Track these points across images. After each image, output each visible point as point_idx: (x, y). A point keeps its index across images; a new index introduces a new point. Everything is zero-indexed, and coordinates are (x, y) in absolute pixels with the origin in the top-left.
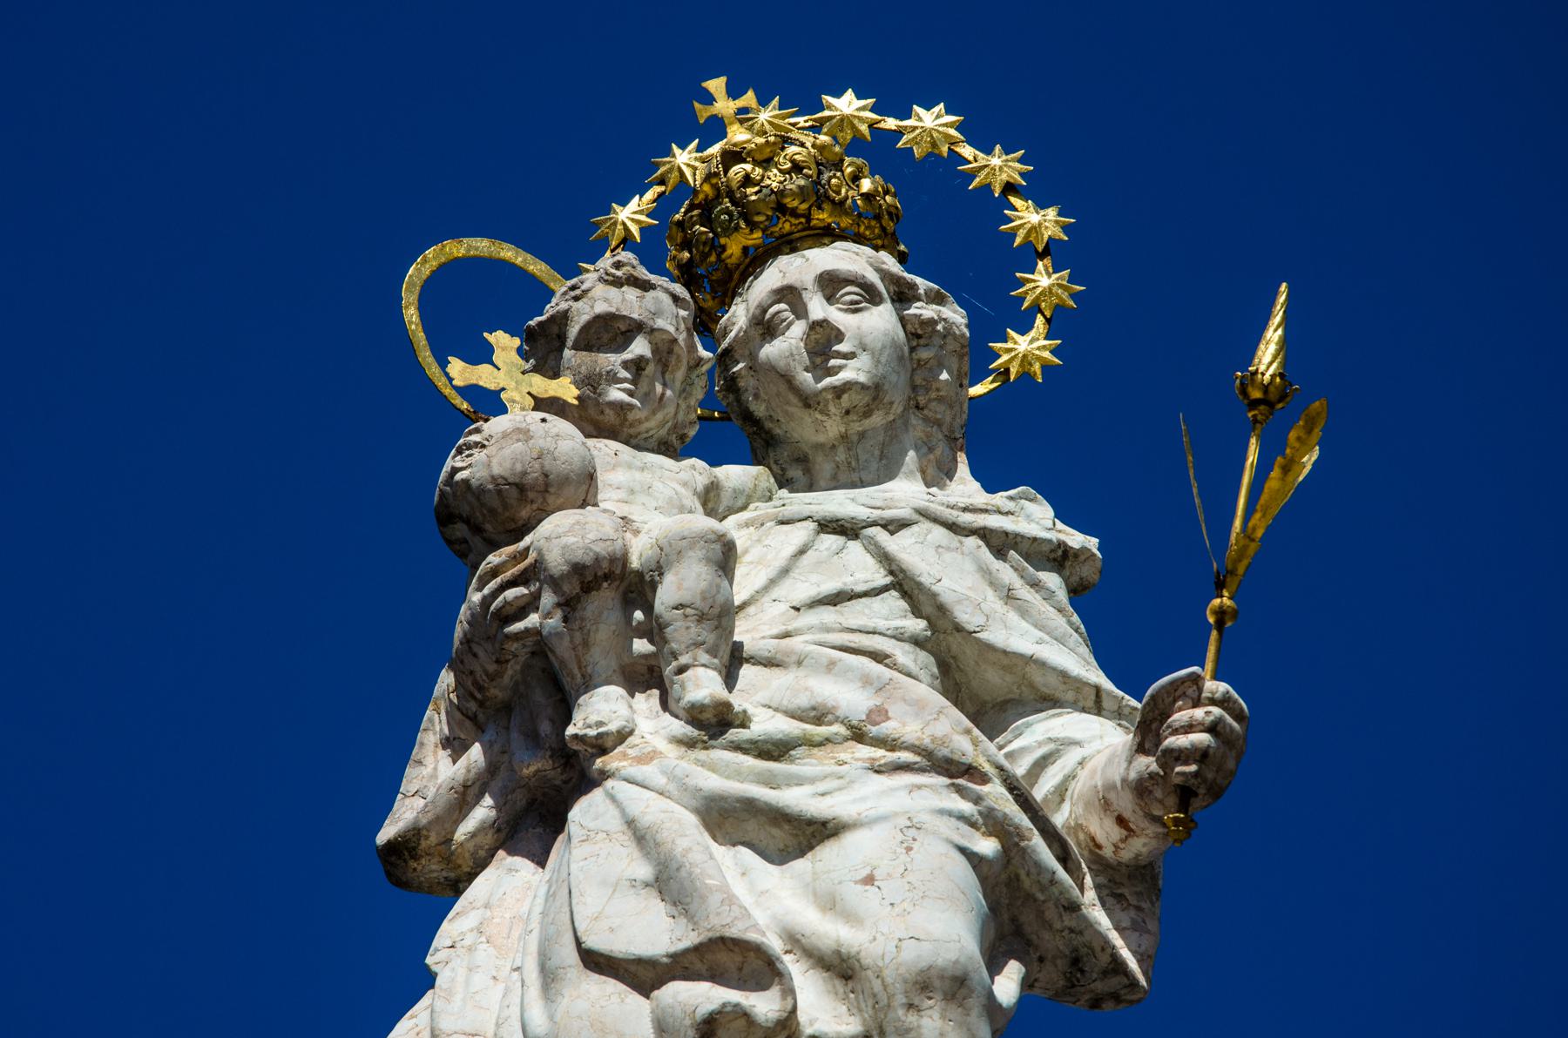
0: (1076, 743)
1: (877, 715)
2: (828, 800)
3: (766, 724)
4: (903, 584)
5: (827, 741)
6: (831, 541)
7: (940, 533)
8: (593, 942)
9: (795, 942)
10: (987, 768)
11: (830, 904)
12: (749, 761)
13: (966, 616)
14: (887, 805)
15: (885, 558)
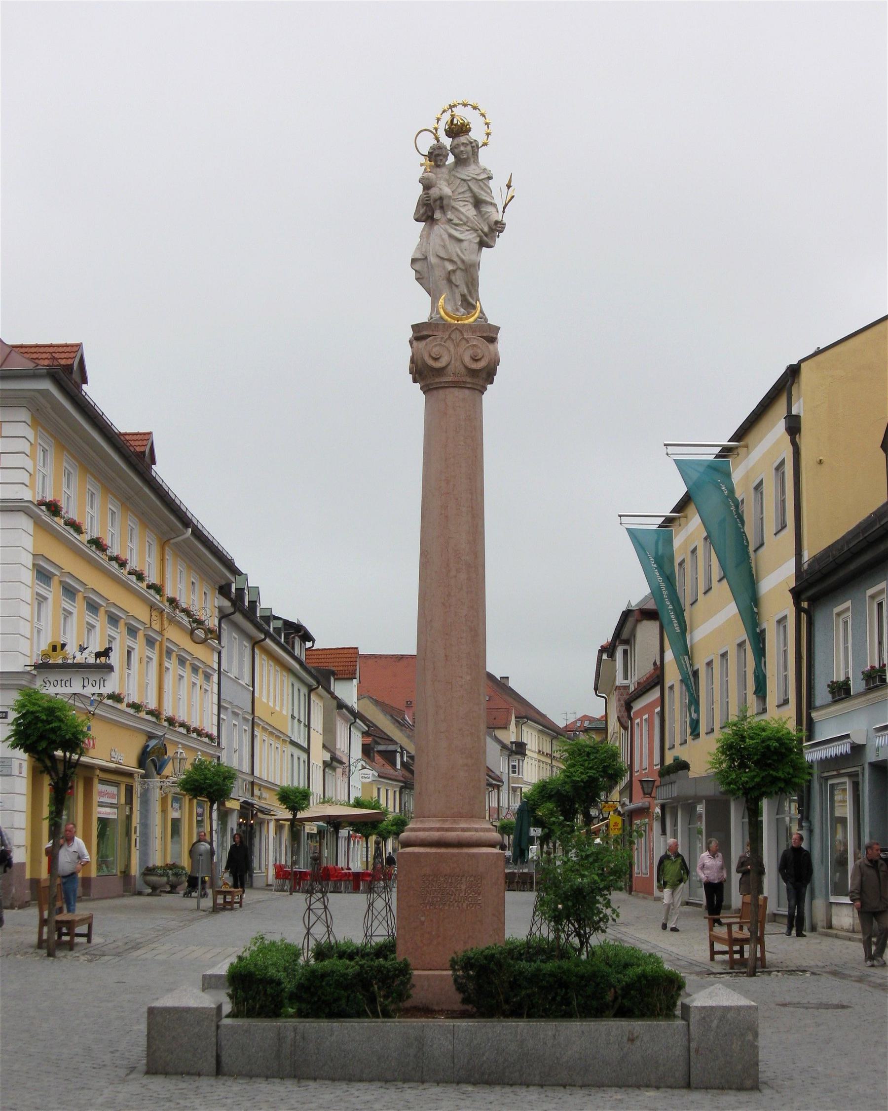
0: (489, 212)
1: (467, 222)
2: (463, 235)
3: (456, 221)
4: (470, 189)
5: (461, 224)
6: (463, 182)
7: (475, 181)
8: (438, 254)
9: (458, 255)
10: (478, 229)
11: (462, 251)
12: (453, 226)
13: (477, 194)
14: (468, 237)
15: (469, 186)
